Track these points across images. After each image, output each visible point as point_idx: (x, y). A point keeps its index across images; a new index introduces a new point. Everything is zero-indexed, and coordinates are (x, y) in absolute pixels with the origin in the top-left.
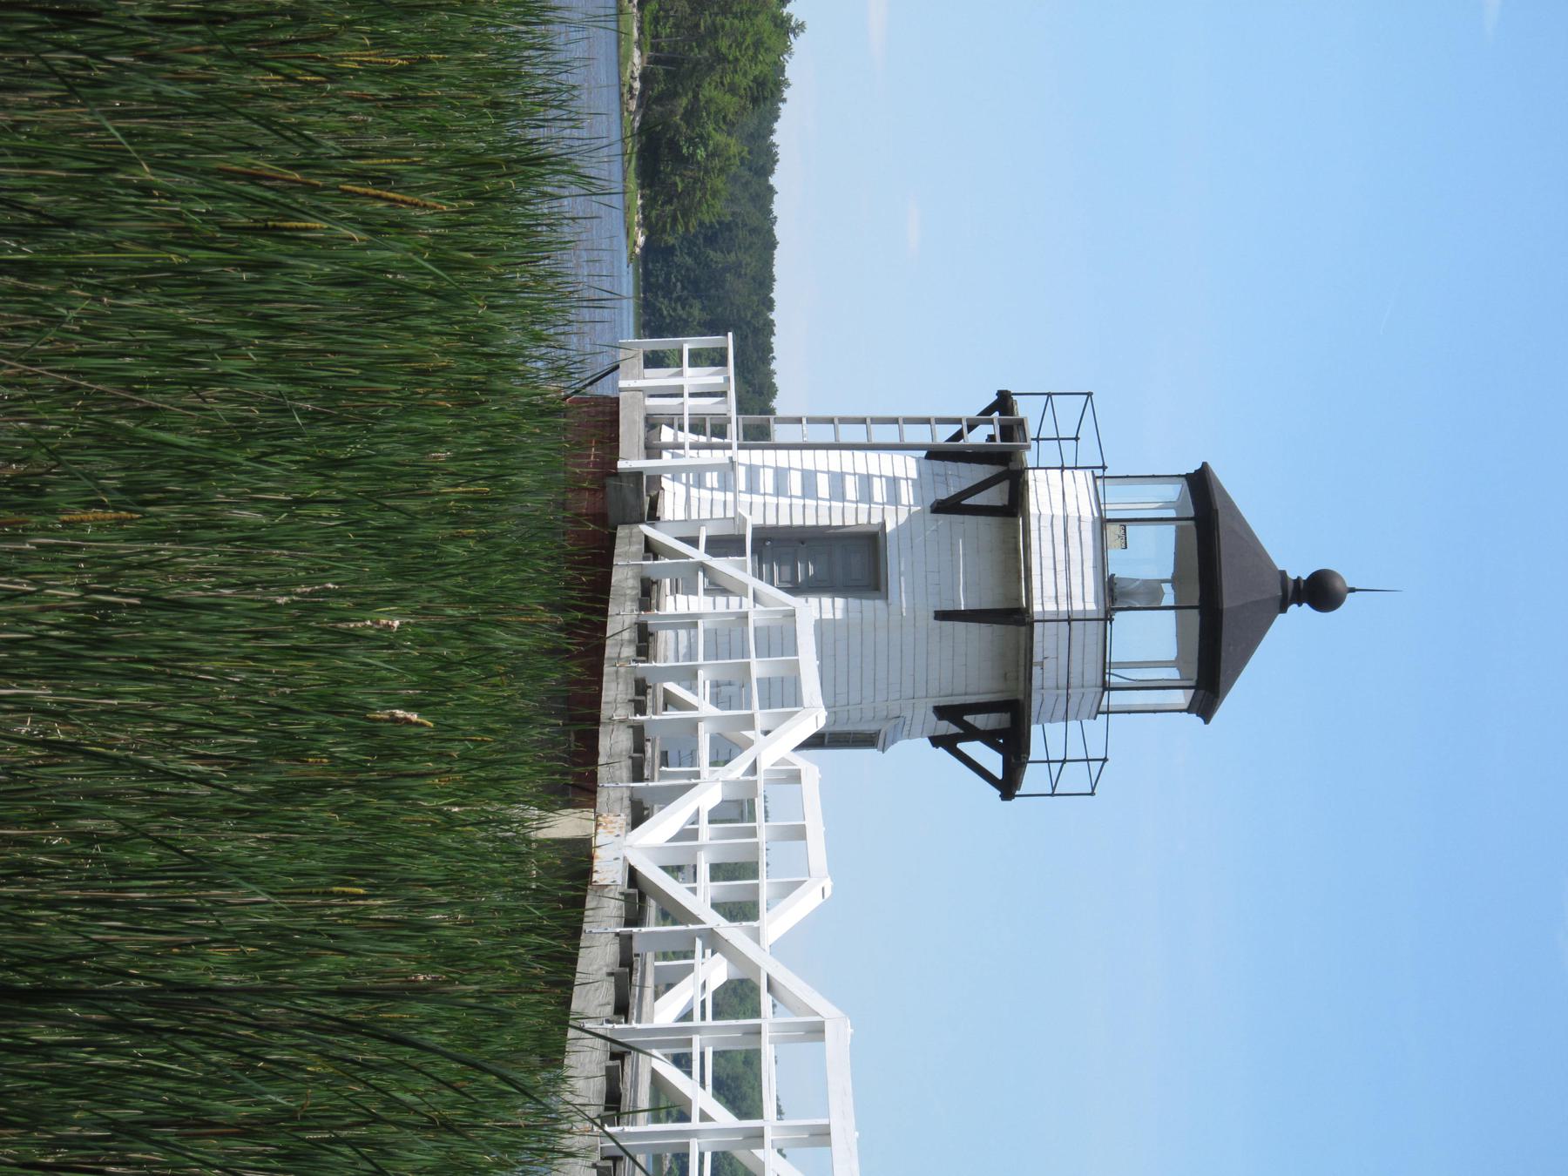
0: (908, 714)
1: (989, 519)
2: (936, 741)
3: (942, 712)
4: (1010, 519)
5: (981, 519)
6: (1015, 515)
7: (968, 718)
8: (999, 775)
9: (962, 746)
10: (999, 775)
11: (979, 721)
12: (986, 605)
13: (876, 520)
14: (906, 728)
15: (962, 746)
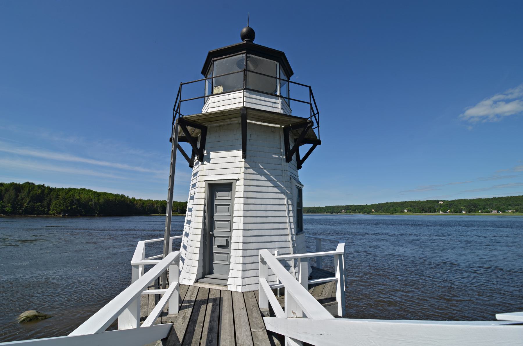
0: (289, 174)
1: (207, 137)
2: (299, 167)
3: (288, 160)
4: (208, 129)
5: (207, 141)
6: (206, 128)
7: (291, 148)
8: (312, 145)
9: (301, 158)
10: (312, 145)
11: (291, 148)
12: (239, 136)
13: (203, 184)
14: (294, 176)
15: (301, 158)
